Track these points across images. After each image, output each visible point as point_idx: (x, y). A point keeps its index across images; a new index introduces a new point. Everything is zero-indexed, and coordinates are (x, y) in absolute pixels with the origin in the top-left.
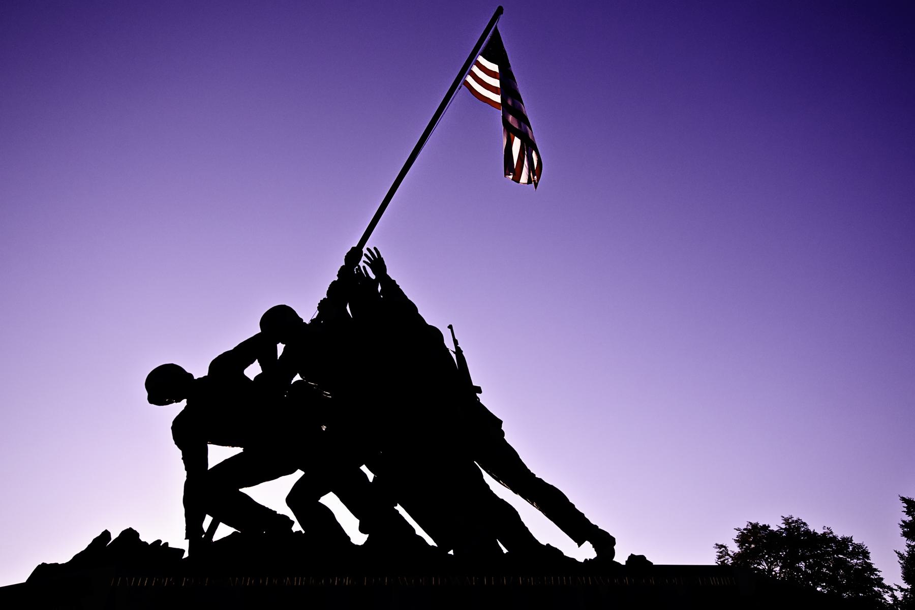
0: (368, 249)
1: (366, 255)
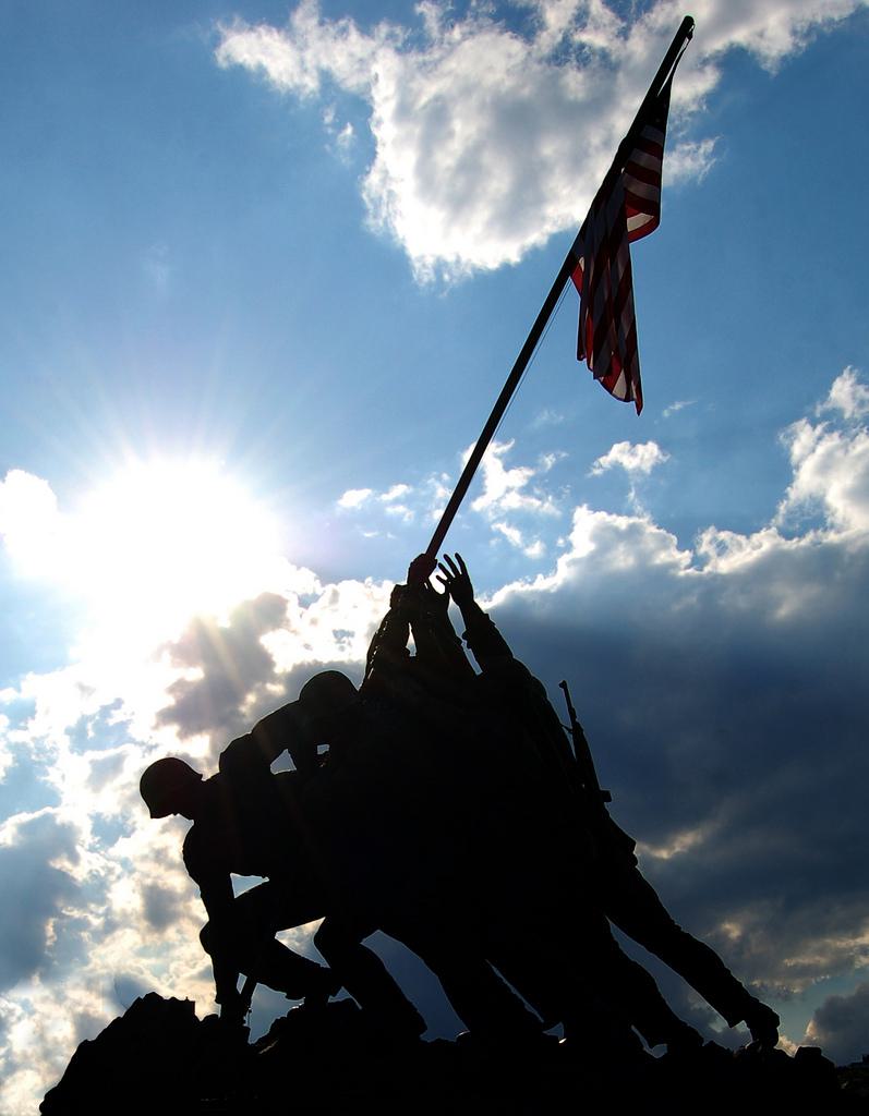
0: (446, 557)
1: (442, 567)
